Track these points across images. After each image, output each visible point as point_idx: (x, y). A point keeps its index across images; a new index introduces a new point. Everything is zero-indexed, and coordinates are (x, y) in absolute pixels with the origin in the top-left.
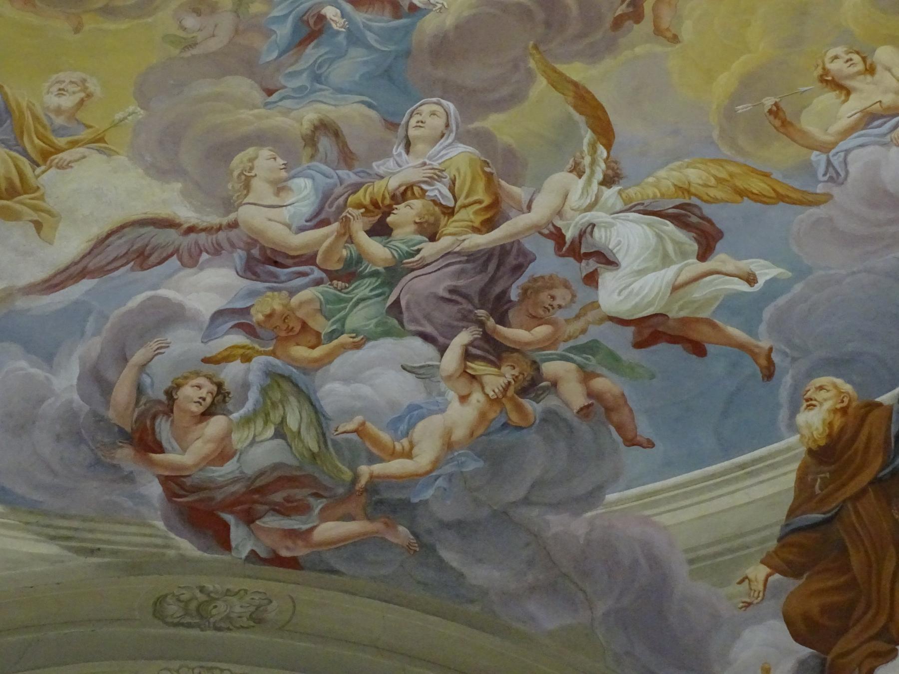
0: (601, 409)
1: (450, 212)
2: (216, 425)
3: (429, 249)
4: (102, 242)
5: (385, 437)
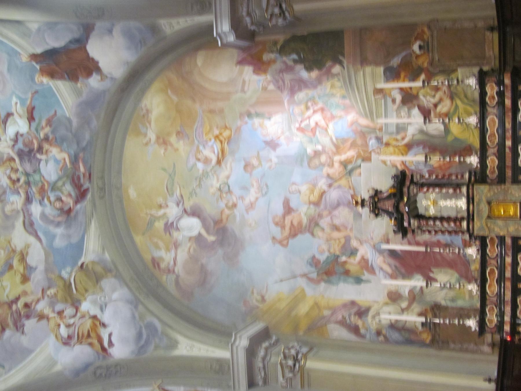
0: (49, 122)
1: (12, 168)
2: (64, 198)
3: (21, 169)
4: (30, 233)
5: (61, 165)
